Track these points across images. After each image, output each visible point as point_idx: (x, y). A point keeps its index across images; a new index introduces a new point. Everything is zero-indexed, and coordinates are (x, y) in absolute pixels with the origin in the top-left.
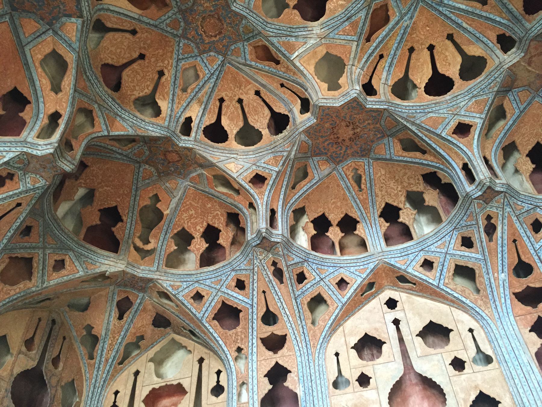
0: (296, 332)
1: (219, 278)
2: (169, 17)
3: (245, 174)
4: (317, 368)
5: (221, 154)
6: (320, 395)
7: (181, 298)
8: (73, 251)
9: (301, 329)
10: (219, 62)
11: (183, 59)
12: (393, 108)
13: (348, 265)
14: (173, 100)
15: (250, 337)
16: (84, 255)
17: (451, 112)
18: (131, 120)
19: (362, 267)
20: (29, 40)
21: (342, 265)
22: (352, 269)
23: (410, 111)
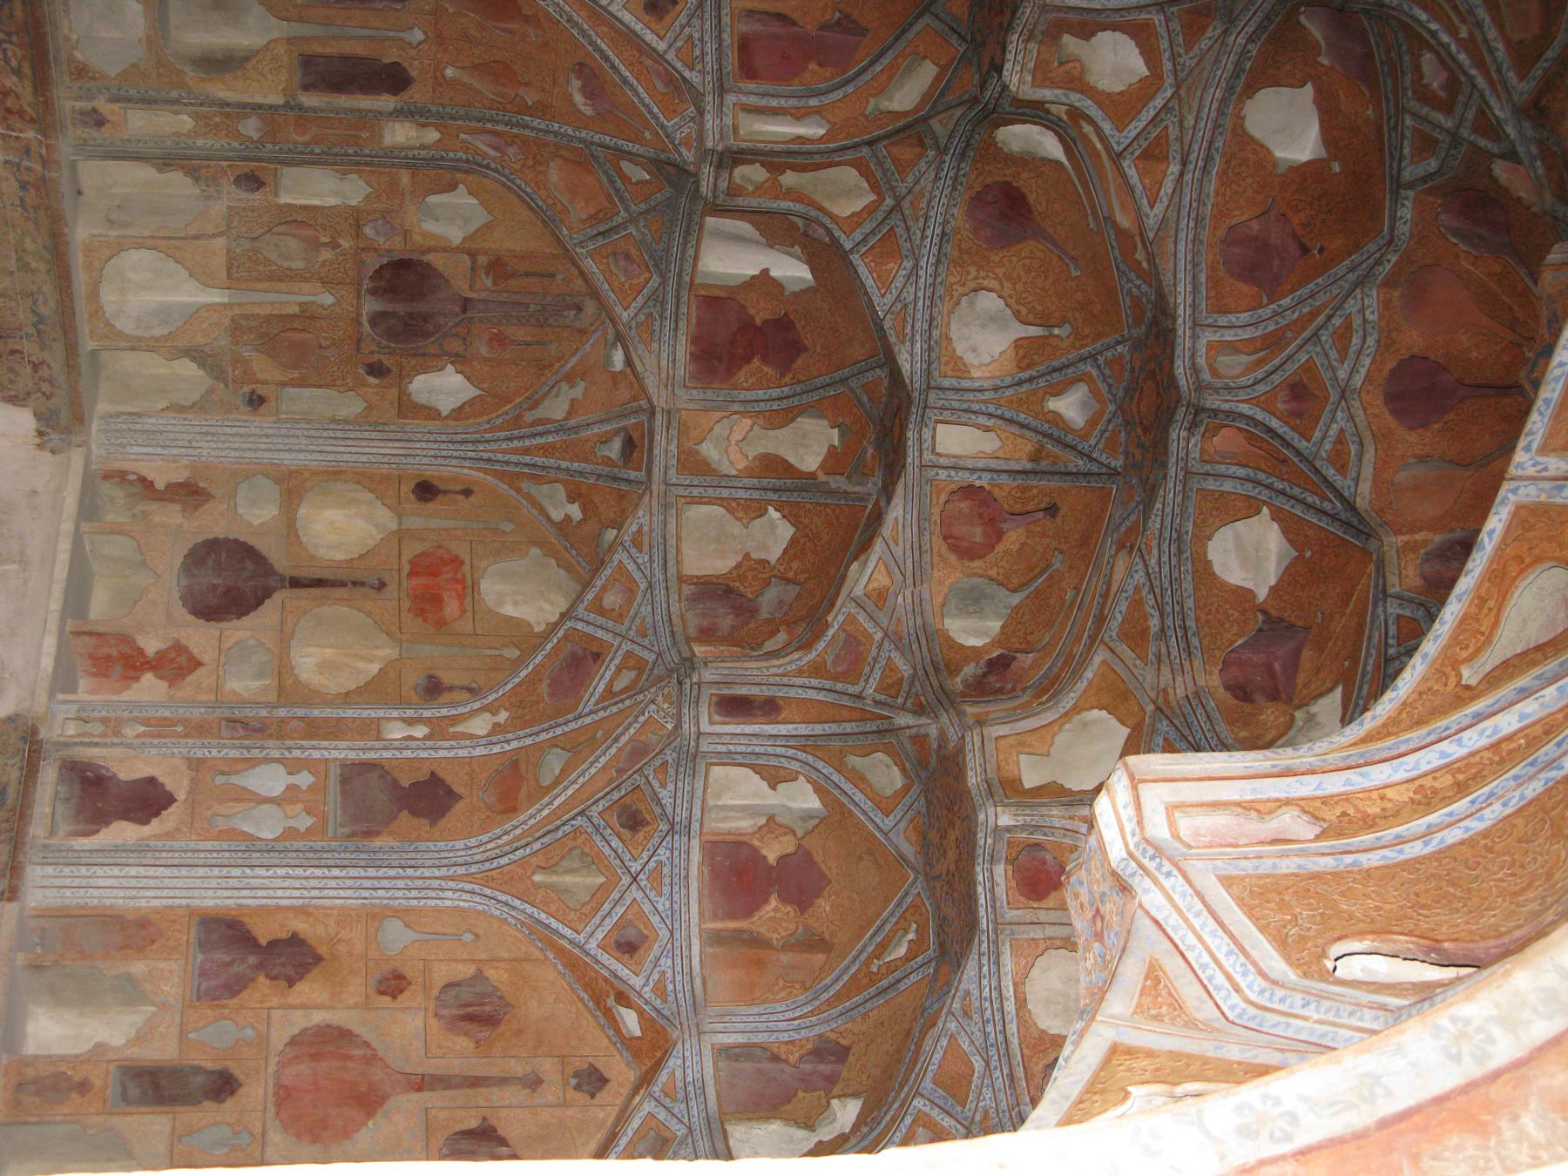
0: (518, 831)
1: (651, 631)
2: (1138, 287)
3: (862, 617)
4: (436, 883)
5: (908, 546)
6: (368, 883)
7: (616, 558)
8: (663, 283)
9: (523, 842)
10: (1113, 464)
11: (1099, 367)
12: (985, 945)
13: (678, 952)
14: (1020, 383)
15: (521, 733)
16: (664, 309)
17: (978, 1118)
18: (920, 294)
19: (670, 987)
20: (942, 15)
21: (677, 935)
22: (666, 963)
23: (987, 1004)
